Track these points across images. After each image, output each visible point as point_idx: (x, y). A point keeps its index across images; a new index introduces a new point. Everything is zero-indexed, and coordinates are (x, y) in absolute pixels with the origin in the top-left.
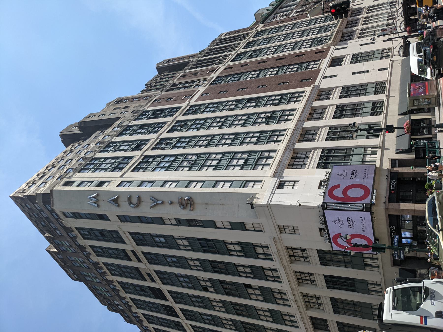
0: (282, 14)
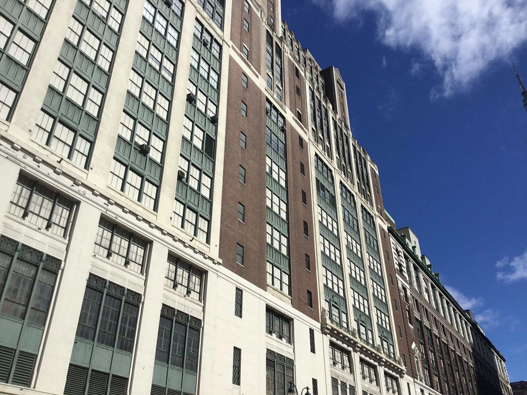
0: (404, 265)
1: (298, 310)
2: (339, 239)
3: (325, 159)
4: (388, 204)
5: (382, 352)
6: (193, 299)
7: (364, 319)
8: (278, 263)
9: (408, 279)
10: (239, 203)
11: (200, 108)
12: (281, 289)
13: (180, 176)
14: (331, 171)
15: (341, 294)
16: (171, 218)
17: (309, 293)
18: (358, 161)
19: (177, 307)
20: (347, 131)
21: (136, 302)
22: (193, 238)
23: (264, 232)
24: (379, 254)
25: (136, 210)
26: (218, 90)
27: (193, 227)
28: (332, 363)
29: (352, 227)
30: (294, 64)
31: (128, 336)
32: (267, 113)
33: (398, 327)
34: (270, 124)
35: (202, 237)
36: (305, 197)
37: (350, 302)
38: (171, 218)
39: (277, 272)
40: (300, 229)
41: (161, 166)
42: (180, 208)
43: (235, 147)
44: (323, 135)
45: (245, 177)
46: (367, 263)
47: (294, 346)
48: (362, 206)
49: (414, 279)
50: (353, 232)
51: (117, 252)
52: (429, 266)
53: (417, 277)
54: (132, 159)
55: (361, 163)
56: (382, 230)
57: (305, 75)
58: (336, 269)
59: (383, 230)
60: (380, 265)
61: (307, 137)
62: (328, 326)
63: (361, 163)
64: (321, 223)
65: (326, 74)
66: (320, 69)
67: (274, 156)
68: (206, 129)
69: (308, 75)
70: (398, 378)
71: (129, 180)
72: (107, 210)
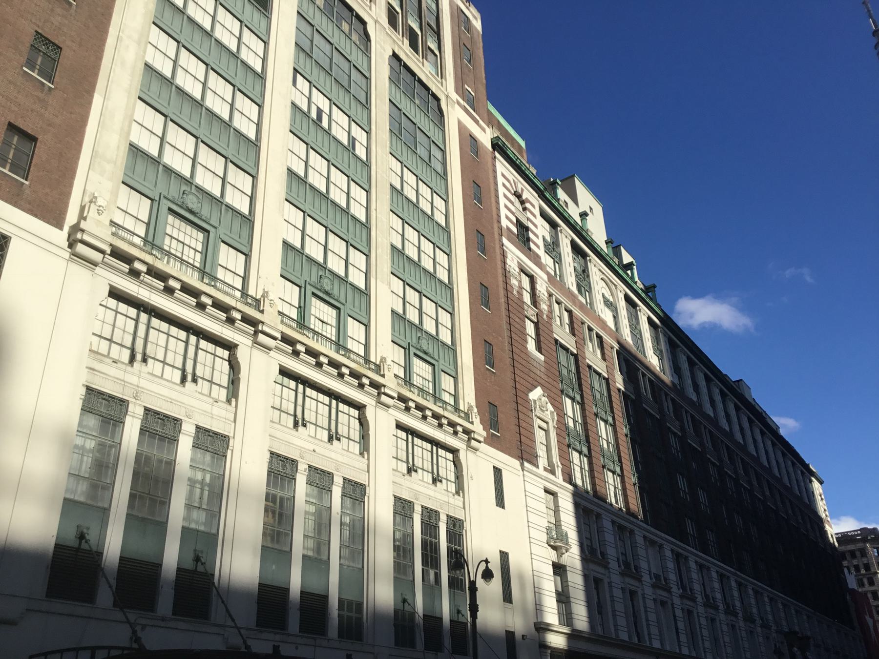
24: (446, 180)
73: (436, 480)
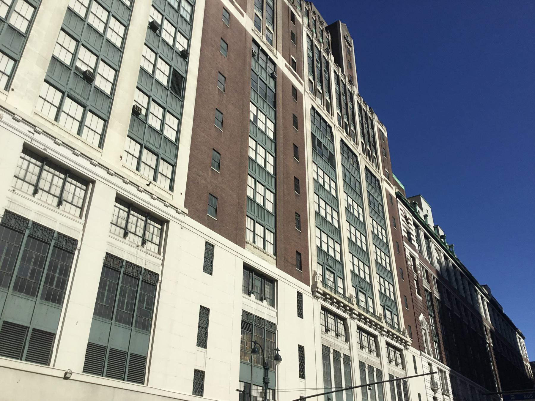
0: (414, 233)
1: (284, 271)
2: (338, 200)
3: (324, 113)
4: (397, 167)
5: (384, 321)
6: (150, 251)
7: (363, 286)
8: (261, 220)
9: (417, 248)
10: (213, 149)
11: (167, 40)
12: (264, 248)
13: (136, 111)
14: (330, 127)
15: (338, 258)
16: (121, 157)
17: (299, 254)
18: (364, 120)
19: (126, 257)
20: (352, 87)
21: (69, 248)
22: (150, 182)
23: (244, 185)
25: (72, 143)
26: (190, 23)
27: (152, 172)
28: (324, 331)
29: (353, 186)
30: (288, 7)
31: (57, 286)
32: (253, 55)
33: (404, 297)
34: (265, 78)
35: (164, 183)
36: (298, 152)
37: (348, 267)
38: (121, 157)
39: (259, 230)
40: (290, 185)
41: (110, 98)
42: (135, 149)
43: (210, 89)
44: (322, 89)
45: (222, 123)
46: (369, 228)
47: (277, 309)
48: (366, 167)
49: (425, 249)
50: (354, 194)
51: (70, 201)
52: (442, 237)
53: (428, 247)
54: (70, 85)
55: (367, 122)
56: (389, 195)
57: (303, 21)
58: (335, 233)
59: (390, 195)
60: (386, 231)
61: (303, 88)
62: (319, 290)
63: (367, 122)
64: (316, 181)
65: (333, 29)
66: (325, 25)
67: (260, 103)
68: (173, 64)
69: (306, 20)
70: (377, 336)
71: (87, 122)
72: (32, 139)
73: (337, 336)
